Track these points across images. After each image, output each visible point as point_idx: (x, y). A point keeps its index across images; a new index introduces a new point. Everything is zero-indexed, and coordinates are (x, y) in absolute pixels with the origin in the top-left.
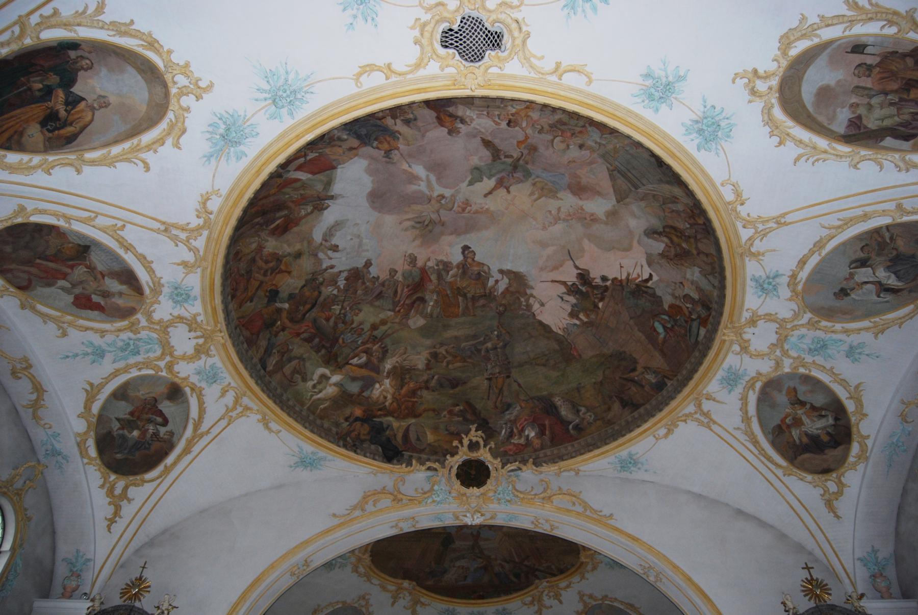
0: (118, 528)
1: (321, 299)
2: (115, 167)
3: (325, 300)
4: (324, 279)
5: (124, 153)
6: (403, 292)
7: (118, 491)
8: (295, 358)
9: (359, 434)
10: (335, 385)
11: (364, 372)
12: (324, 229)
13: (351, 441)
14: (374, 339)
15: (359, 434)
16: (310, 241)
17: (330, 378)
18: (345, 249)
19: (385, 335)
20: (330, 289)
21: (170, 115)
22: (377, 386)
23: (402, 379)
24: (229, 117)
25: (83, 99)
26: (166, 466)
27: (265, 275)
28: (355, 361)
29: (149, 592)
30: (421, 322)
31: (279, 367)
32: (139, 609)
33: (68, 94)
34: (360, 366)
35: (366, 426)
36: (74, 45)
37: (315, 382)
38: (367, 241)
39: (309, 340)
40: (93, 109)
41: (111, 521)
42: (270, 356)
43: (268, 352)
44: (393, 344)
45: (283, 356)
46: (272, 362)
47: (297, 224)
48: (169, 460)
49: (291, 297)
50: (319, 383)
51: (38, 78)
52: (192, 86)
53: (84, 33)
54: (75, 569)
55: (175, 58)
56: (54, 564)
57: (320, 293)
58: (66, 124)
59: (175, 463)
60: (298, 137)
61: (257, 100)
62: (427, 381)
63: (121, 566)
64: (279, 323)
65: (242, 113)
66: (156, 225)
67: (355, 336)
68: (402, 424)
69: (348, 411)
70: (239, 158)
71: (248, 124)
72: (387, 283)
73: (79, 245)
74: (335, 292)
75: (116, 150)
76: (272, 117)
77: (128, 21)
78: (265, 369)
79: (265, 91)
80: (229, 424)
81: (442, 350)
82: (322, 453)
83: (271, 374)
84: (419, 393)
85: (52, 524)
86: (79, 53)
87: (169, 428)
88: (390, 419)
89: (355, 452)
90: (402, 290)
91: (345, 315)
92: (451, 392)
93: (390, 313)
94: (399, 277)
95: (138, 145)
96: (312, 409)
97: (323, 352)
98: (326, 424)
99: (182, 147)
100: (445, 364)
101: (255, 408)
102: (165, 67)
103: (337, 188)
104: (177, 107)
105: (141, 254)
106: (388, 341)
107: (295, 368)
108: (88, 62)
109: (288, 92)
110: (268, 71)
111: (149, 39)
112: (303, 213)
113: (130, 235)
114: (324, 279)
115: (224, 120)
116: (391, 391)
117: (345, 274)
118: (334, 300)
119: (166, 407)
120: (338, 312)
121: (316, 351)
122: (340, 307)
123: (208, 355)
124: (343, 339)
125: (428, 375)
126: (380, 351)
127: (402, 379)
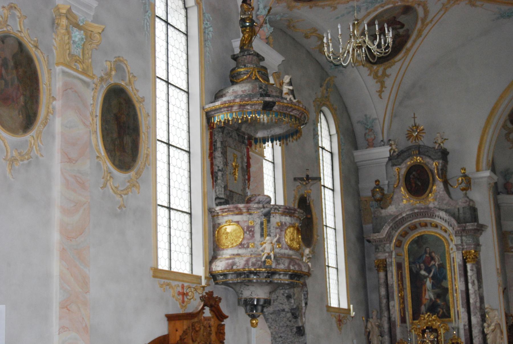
0: (386, 94)
7: (380, 73)
26: (407, 49)
29: (425, 133)
32: (423, 145)
48: (408, 45)
54: (368, 127)
56: (352, 125)
59: (412, 45)
80: (445, 12)
85: (344, 104)
87: (405, 28)
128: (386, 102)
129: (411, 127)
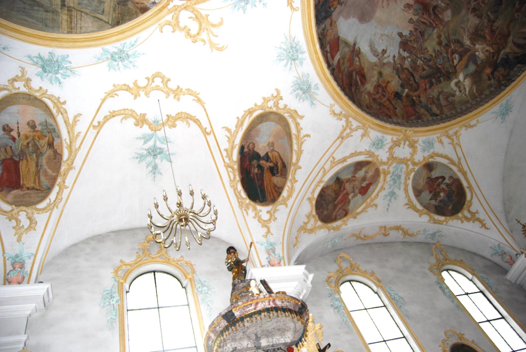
0: (489, 224)
1: (410, 69)
2: (303, 151)
3: (411, 67)
4: (400, 64)
5: (297, 144)
6: (425, 18)
7: (469, 216)
8: (439, 96)
9: (503, 75)
10: (465, 79)
11: (465, 58)
12: (371, 54)
13: (505, 82)
14: (448, 46)
15: (503, 75)
16: (375, 65)
17: (459, 81)
18: (387, 46)
19: (448, 38)
20: (406, 62)
21: (286, 115)
22: (477, 53)
23: (480, 36)
24: (295, 86)
25: (267, 153)
26: (468, 188)
27: (384, 96)
28: (456, 62)
30: (449, 13)
31: (439, 106)
33: (263, 158)
34: (460, 59)
35: (500, 69)
36: (242, 148)
37: (458, 90)
38: (386, 31)
39: (431, 85)
40: (273, 150)
41: (484, 225)
42: (431, 110)
43: (429, 110)
44: (455, 35)
45: (435, 103)
46: (435, 109)
47: (363, 69)
48: (465, 184)
49: (402, 86)
50: (459, 88)
51: (253, 169)
52: (275, 100)
53: (238, 141)
54: (500, 253)
55: (259, 104)
57: (407, 69)
58: (276, 165)
59: (468, 182)
60: (316, 53)
61: (290, 69)
62: (489, 21)
63: (511, 232)
64: (414, 98)
65: (295, 79)
66: (338, 142)
67: (440, 56)
68: (509, 45)
69: (485, 77)
70: (318, 88)
71: (301, 77)
72: (416, 27)
73: (335, 181)
74: (409, 60)
75: (295, 147)
76: (301, 63)
77: (237, 120)
78: (438, 115)
79: (287, 63)
80: (460, 146)
81: (473, 4)
82: (503, 101)
83: (442, 112)
84: (494, 28)
85: (469, 252)
86: (246, 147)
88: (502, 52)
89: (513, 81)
90: (425, 19)
91: (425, 58)
92: (503, 6)
93: (435, 31)
94: (415, 18)
95: (296, 136)
96: (474, 97)
97: (442, 79)
98: (487, 92)
99: (303, 115)
100: (483, 5)
101: (457, 129)
102: (262, 110)
103: (350, 40)
104: (283, 111)
105: (350, 155)
106: (452, 38)
107: (444, 98)
108: (251, 144)
109: (291, 51)
110: (277, 58)
111: (248, 113)
112: (358, 63)
113: (338, 156)
114: (400, 64)
115: (296, 89)
116: (485, 45)
117: (401, 51)
118: (414, 62)
119: (435, 174)
120: (422, 62)
121: (440, 83)
122: (419, 60)
123: (416, 142)
124: (439, 64)
125: (485, 18)
126: (456, 44)
127: (480, 36)
128: (495, 228)
129: (523, 229)
